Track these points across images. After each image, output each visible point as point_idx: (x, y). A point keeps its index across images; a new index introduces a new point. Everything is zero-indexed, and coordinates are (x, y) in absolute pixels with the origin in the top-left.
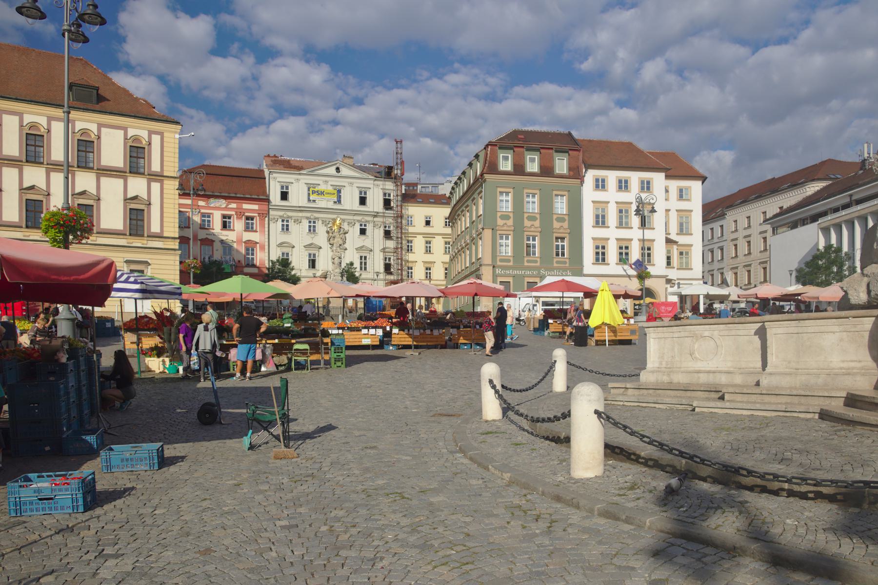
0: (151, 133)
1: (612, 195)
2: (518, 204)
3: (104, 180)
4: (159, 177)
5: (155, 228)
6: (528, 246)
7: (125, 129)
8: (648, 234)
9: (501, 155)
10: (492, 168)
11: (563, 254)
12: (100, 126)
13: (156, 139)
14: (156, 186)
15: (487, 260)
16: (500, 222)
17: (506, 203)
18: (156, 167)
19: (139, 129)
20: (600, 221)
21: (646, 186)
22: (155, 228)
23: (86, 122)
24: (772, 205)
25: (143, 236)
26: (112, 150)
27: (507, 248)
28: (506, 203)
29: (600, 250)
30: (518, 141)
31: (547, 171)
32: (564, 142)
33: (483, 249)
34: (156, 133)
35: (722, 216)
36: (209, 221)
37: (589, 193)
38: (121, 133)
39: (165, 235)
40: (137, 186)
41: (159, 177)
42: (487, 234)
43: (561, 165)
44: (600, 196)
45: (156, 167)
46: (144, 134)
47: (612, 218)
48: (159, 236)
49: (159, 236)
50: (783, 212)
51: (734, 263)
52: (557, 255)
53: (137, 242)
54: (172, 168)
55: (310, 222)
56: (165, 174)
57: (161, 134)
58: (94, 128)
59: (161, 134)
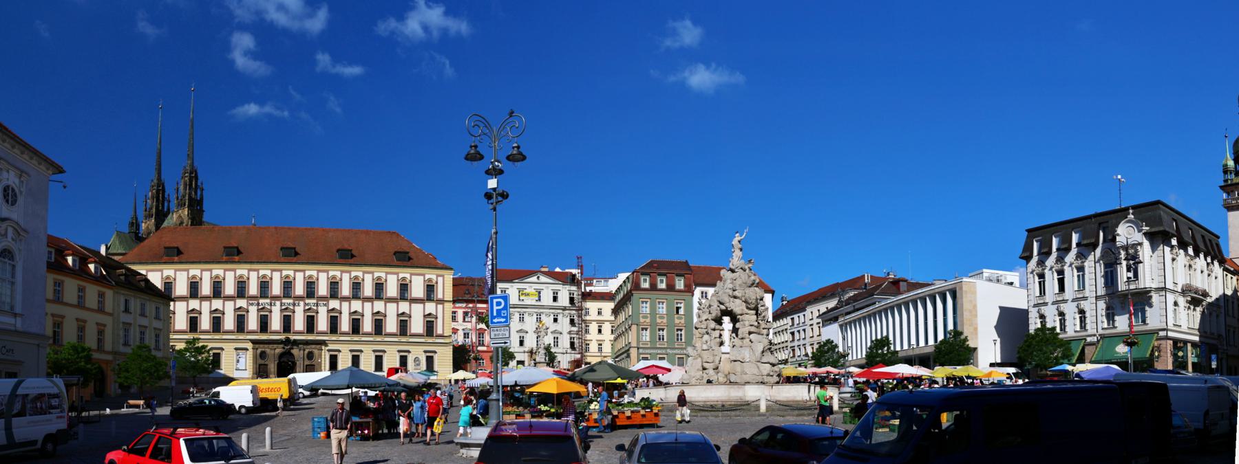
2: (653, 309)
4: (442, 302)
5: (440, 331)
9: (642, 278)
10: (636, 286)
13: (440, 279)
14: (440, 307)
15: (634, 344)
16: (642, 320)
17: (646, 309)
19: (431, 275)
23: (405, 273)
24: (823, 307)
27: (646, 336)
28: (646, 309)
30: (654, 268)
31: (671, 288)
32: (682, 268)
33: (632, 337)
35: (804, 309)
40: (430, 307)
41: (442, 302)
42: (634, 328)
43: (680, 284)
45: (440, 296)
46: (434, 277)
50: (829, 311)
51: (802, 342)
54: (449, 296)
58: (408, 276)
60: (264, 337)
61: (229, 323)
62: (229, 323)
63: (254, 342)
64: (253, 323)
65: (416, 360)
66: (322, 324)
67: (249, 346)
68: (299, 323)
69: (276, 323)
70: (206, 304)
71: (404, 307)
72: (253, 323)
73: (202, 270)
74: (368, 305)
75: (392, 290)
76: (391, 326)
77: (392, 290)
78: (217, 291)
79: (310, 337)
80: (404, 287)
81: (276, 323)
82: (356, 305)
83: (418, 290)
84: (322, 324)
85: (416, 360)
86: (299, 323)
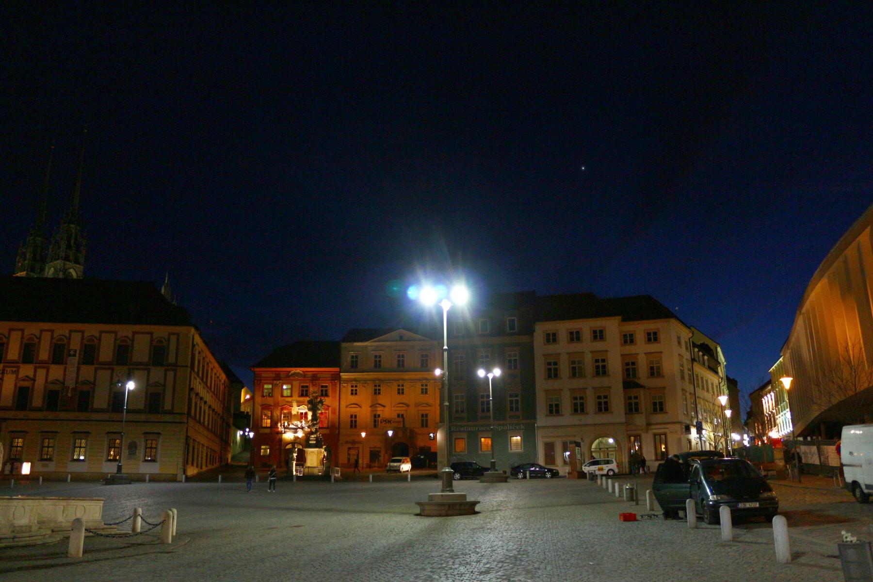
1: (563, 347)
6: (483, 403)
8: (605, 381)
11: (517, 409)
13: (173, 339)
18: (171, 359)
20: (553, 373)
21: (599, 335)
22: (168, 406)
26: (141, 349)
29: (579, 401)
34: (174, 334)
38: (148, 337)
44: (552, 349)
47: (564, 369)
49: (171, 413)
52: (511, 409)
53: (153, 417)
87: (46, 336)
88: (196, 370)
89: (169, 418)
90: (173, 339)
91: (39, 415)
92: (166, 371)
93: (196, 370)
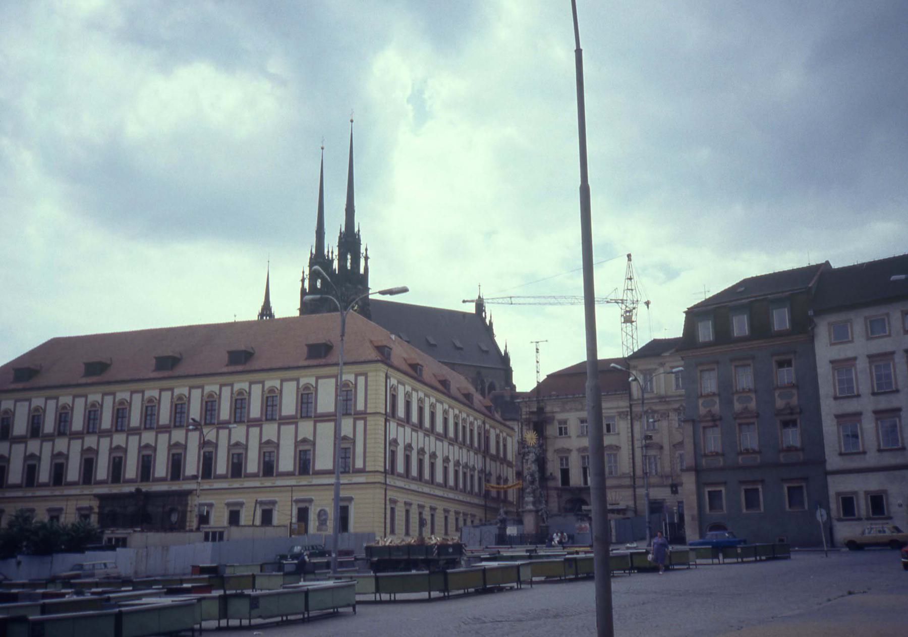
0: (357, 376)
3: (319, 425)
4: (362, 416)
5: (359, 464)
7: (336, 376)
12: (318, 378)
13: (361, 379)
14: (360, 424)
18: (360, 406)
22: (359, 464)
23: (308, 379)
25: (349, 472)
34: (361, 374)
36: (566, 428)
37: (825, 351)
39: (367, 469)
41: (362, 416)
45: (360, 406)
48: (362, 471)
49: (362, 471)
55: (679, 414)
56: (369, 411)
57: (365, 375)
59: (365, 375)
60: (115, 489)
61: (73, 473)
62: (73, 473)
63: (101, 498)
64: (102, 471)
65: (322, 514)
66: (191, 466)
67: (95, 504)
68: (161, 468)
69: (131, 470)
70: (47, 446)
71: (306, 428)
72: (102, 471)
73: (47, 399)
74: (254, 431)
75: (289, 406)
76: (286, 461)
77: (289, 406)
78: (63, 428)
79: (175, 487)
80: (306, 399)
81: (131, 470)
82: (239, 433)
83: (326, 401)
84: (191, 466)
85: (322, 514)
86: (161, 468)
87: (226, 392)
88: (401, 413)
89: (361, 479)
90: (361, 379)
91: (224, 485)
92: (355, 420)
93: (401, 413)
